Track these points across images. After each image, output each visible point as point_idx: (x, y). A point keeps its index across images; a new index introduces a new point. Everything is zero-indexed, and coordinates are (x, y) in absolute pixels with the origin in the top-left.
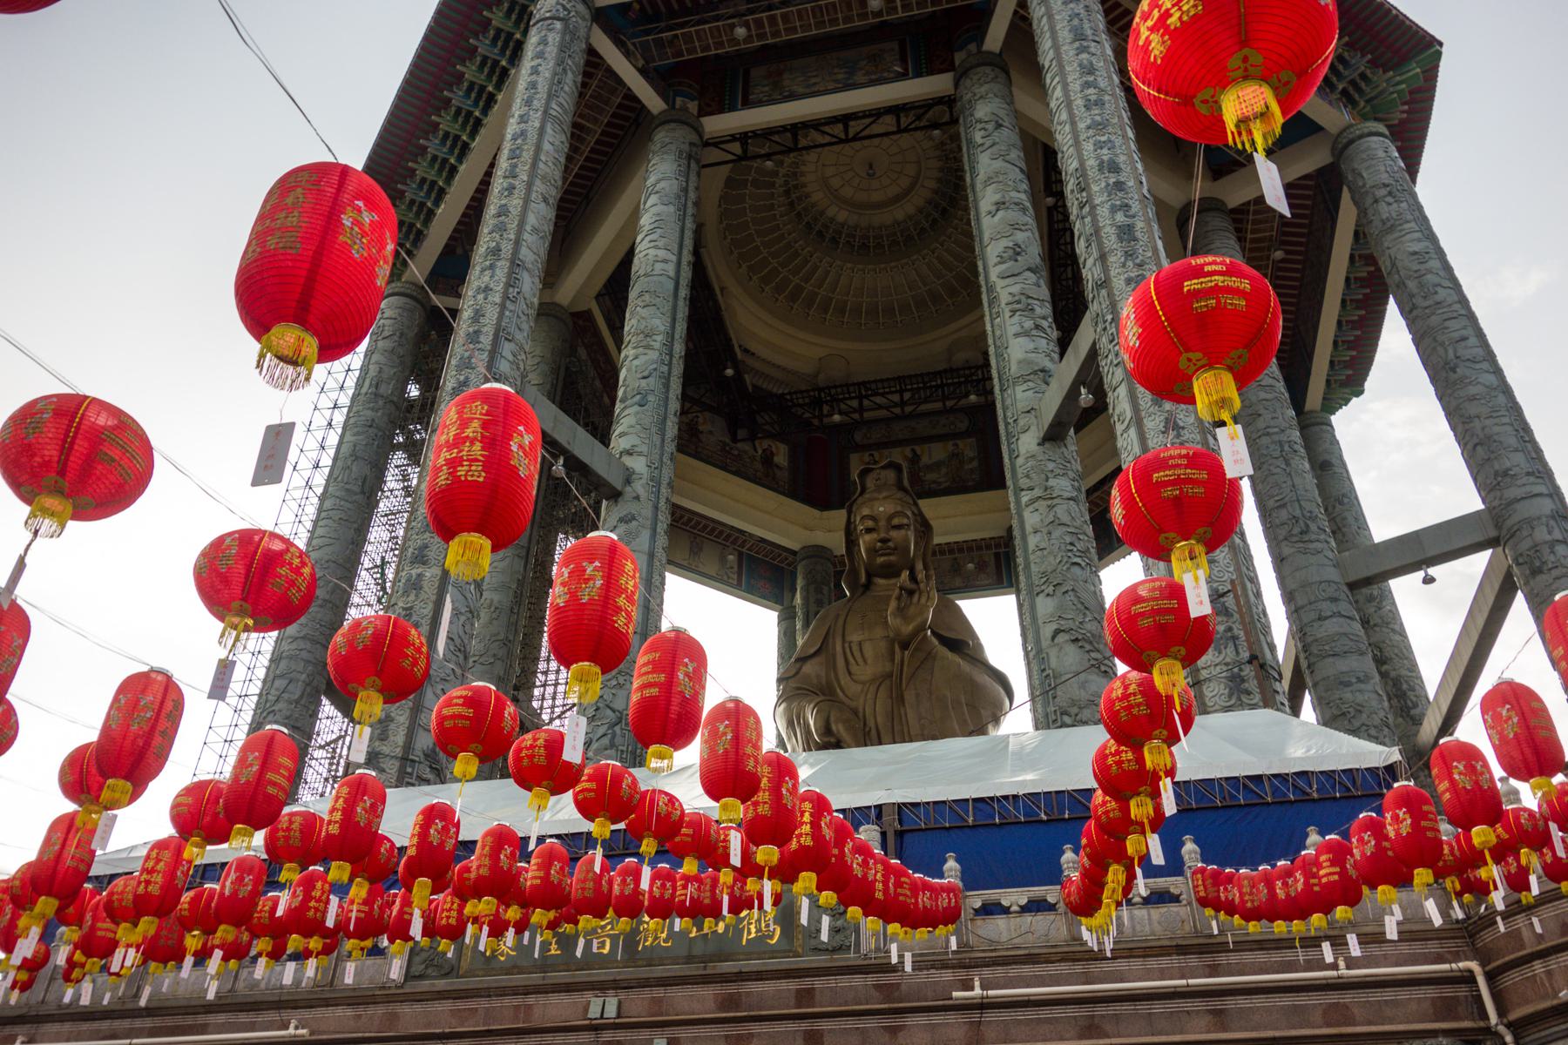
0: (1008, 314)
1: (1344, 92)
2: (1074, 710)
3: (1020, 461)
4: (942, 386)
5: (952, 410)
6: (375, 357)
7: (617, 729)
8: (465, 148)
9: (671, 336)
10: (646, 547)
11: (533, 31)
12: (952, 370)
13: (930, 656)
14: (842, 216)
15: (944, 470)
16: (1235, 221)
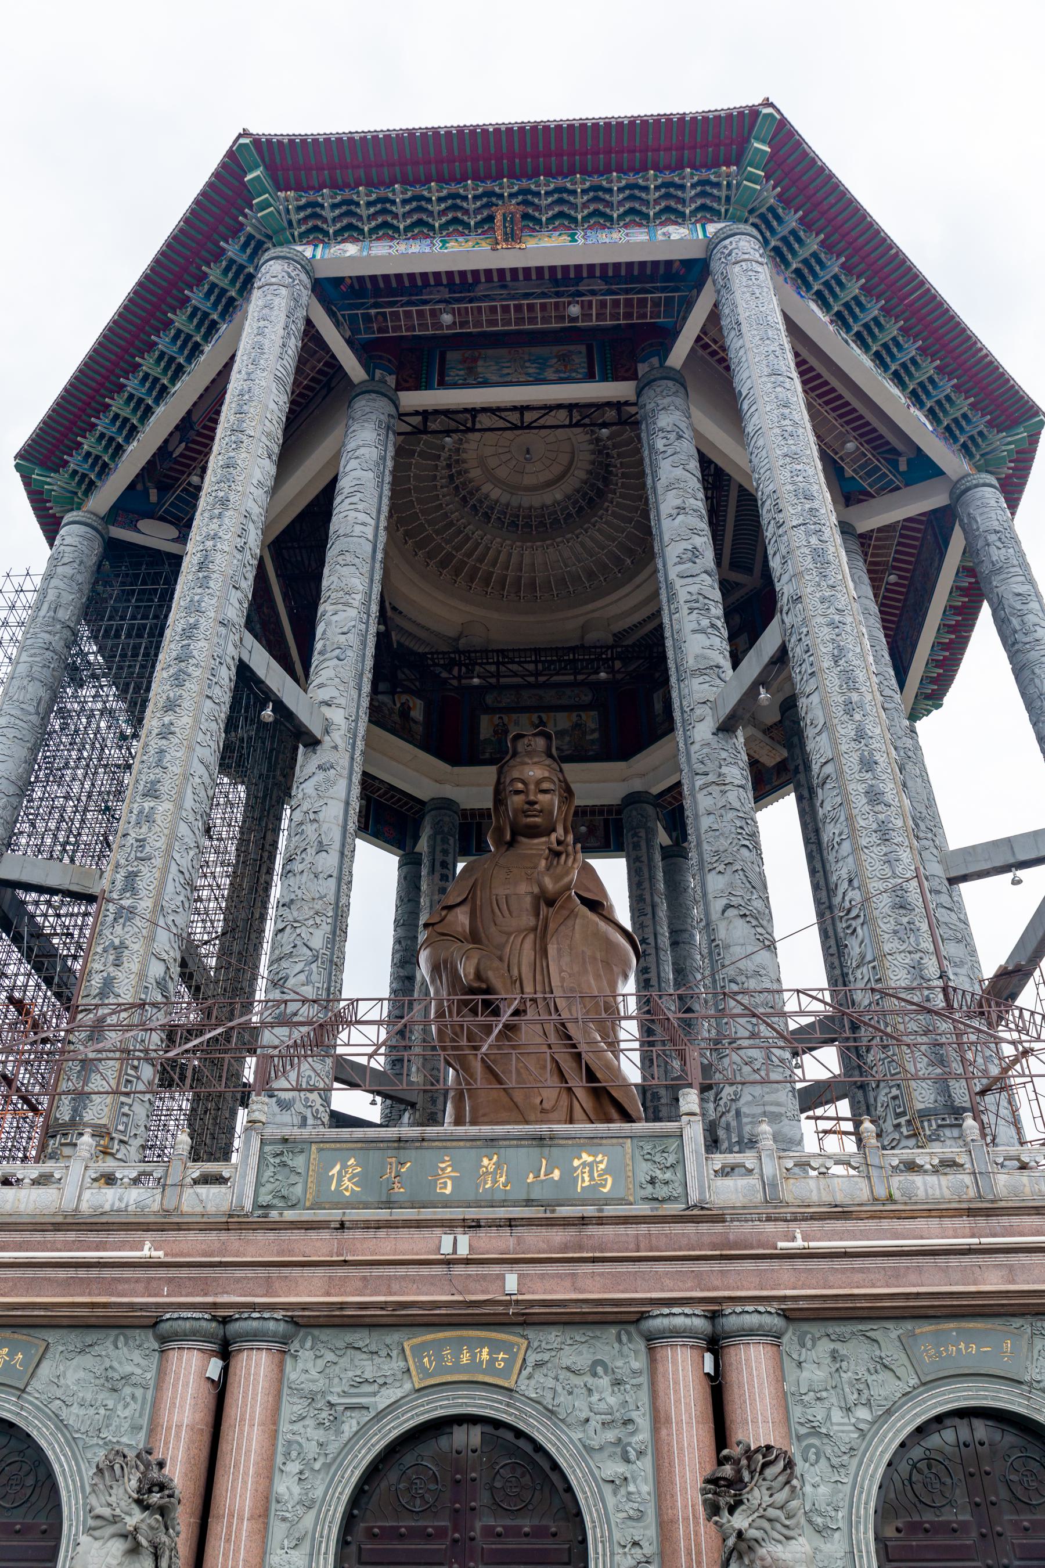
0: (686, 611)
1: (964, 446)
2: (739, 979)
3: (694, 748)
4: (574, 661)
5: (582, 684)
6: (54, 582)
7: (314, 966)
8: (164, 389)
9: (369, 595)
10: (343, 795)
11: (256, 294)
12: (582, 646)
13: (572, 914)
14: (495, 494)
15: (567, 739)
16: (862, 545)
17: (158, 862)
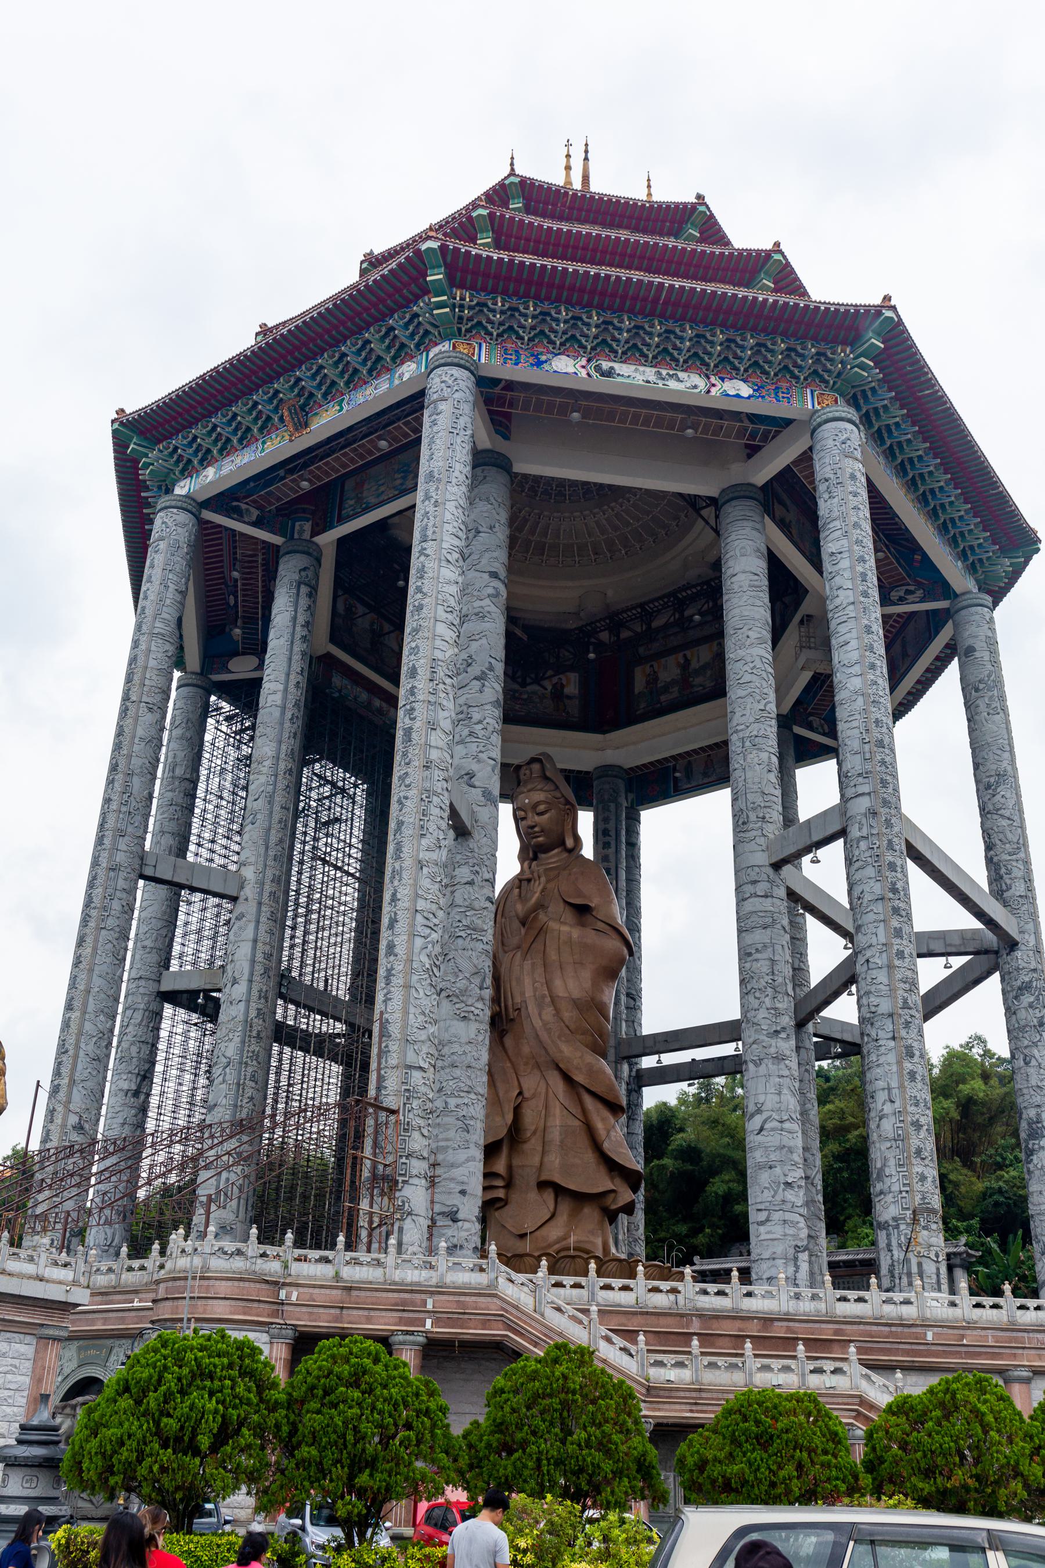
15: (709, 673)
17: (71, 1053)
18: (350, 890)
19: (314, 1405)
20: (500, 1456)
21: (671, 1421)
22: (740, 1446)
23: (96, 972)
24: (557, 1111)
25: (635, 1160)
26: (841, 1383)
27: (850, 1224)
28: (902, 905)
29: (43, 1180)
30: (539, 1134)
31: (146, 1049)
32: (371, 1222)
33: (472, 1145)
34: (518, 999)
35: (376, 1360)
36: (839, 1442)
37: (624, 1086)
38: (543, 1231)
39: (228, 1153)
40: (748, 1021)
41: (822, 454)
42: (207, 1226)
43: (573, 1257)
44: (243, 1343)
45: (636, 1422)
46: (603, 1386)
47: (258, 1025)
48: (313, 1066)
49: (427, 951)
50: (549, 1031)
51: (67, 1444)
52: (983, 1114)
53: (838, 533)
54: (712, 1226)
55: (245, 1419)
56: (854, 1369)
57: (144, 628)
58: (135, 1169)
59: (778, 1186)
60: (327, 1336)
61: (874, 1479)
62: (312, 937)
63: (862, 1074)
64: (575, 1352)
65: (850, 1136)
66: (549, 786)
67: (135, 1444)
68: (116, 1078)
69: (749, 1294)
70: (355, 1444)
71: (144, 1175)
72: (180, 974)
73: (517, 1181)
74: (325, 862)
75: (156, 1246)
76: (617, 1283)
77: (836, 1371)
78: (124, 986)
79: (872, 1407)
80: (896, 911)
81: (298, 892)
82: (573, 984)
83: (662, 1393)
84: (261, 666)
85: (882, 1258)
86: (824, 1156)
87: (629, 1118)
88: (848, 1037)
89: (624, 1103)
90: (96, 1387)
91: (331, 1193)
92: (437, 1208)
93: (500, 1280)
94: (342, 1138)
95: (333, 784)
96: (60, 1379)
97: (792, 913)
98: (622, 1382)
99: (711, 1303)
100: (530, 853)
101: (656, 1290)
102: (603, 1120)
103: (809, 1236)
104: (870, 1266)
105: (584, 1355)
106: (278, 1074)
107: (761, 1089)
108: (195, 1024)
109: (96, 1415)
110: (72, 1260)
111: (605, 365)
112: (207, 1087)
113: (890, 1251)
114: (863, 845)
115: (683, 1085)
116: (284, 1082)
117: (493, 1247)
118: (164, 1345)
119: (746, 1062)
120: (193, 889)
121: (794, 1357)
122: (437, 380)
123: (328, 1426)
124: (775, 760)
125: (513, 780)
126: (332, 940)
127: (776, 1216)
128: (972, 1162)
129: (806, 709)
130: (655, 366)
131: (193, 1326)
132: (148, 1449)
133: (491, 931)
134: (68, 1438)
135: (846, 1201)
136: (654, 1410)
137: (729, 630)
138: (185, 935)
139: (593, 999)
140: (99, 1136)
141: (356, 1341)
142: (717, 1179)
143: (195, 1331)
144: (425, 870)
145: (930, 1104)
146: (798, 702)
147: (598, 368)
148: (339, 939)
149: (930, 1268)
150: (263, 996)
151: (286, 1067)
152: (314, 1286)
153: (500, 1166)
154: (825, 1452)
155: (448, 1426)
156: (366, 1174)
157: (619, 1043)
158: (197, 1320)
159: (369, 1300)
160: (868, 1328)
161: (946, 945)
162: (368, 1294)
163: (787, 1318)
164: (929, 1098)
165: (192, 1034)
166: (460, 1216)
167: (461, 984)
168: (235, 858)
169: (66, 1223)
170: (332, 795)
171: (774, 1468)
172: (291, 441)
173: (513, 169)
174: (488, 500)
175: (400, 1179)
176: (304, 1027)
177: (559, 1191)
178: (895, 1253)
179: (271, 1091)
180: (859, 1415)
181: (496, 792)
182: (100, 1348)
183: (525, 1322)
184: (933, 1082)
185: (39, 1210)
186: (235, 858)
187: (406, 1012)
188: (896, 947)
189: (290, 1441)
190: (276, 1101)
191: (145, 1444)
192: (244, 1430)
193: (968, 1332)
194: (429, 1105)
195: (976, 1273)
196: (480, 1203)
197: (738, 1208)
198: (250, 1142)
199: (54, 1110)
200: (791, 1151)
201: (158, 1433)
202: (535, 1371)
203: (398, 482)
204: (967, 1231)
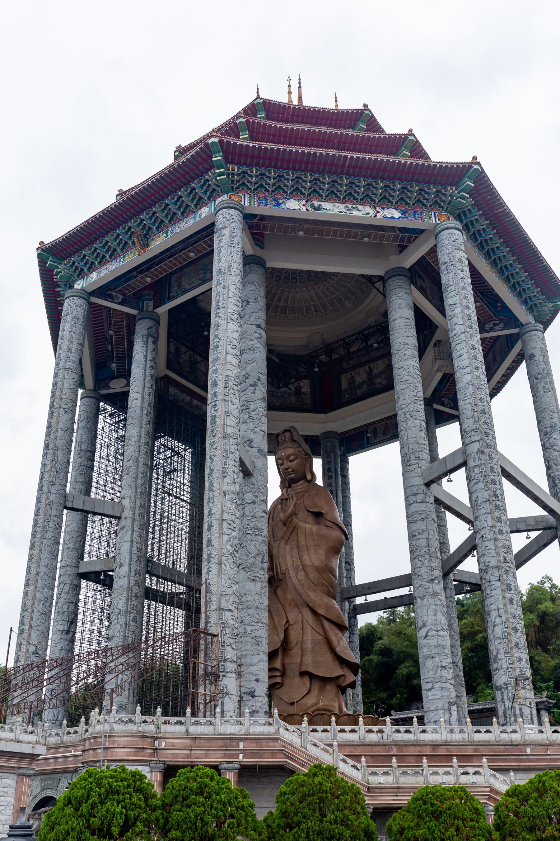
7: (119, 616)
18: (185, 510)
19: (178, 806)
20: (285, 831)
21: (382, 806)
22: (423, 819)
23: (42, 564)
24: (309, 631)
25: (355, 657)
26: (479, 780)
27: (480, 688)
28: (500, 504)
29: (16, 684)
30: (299, 644)
31: (72, 606)
32: (205, 700)
33: (261, 653)
34: (283, 568)
35: (212, 779)
36: (480, 814)
37: (346, 615)
38: (304, 701)
39: (122, 664)
40: (416, 574)
41: (442, 248)
42: (111, 706)
43: (322, 714)
44: (135, 772)
45: (363, 808)
46: (343, 788)
47: (135, 589)
48: (168, 611)
49: (230, 543)
50: (302, 585)
51: (37, 835)
52: (552, 621)
53: (453, 293)
54: (401, 693)
55: (138, 816)
56: (486, 771)
57: (61, 365)
58: (69, 676)
59: (438, 668)
60: (183, 767)
61: (501, 834)
62: (164, 538)
63: (482, 602)
64: (326, 769)
65: (477, 638)
66: (296, 445)
67: (76, 834)
68: (55, 624)
69: (424, 731)
70: (202, 828)
71: (74, 679)
72: (90, 562)
73: (288, 672)
74: (170, 494)
75: (83, 719)
76: (348, 728)
77: (475, 773)
78: (58, 571)
79: (497, 793)
80: (497, 507)
81: (155, 512)
82: (314, 558)
83: (376, 790)
84: (128, 384)
85: (499, 706)
86: (463, 650)
87: (350, 633)
88: (473, 581)
89: (347, 624)
90: (52, 802)
91: (182, 684)
92: (243, 690)
93: (281, 729)
94: (186, 652)
95: (172, 450)
96: (31, 798)
97: (438, 511)
98: (353, 785)
99: (402, 737)
100: (286, 484)
101: (370, 731)
102: (335, 635)
103: (457, 696)
104: (492, 712)
105: (331, 771)
106: (148, 617)
107: (425, 613)
108: (100, 591)
109: (53, 819)
110: (35, 730)
111: (316, 204)
112: (108, 626)
113: (503, 702)
114: (477, 470)
115: (381, 613)
116: (152, 622)
117: (276, 711)
118: (90, 776)
119: (415, 598)
120: (95, 514)
121: (451, 766)
122: (221, 217)
123: (186, 818)
124: (424, 424)
125: (274, 443)
126: (176, 539)
127: (437, 685)
128: (548, 649)
129: (440, 394)
130: (345, 203)
131: (106, 764)
132: (83, 836)
133: (266, 530)
134: (37, 832)
135: (476, 674)
136: (373, 800)
137: (394, 351)
138: (91, 540)
139: (326, 566)
140: (48, 658)
141: (200, 769)
142: (402, 666)
143: (107, 767)
144: (227, 496)
145: (522, 617)
146: (435, 391)
147: (312, 206)
148: (180, 538)
149: (526, 711)
150: (138, 573)
151: (153, 613)
152: (174, 738)
153: (278, 664)
154: (472, 820)
155: (255, 815)
156: (201, 672)
157: (343, 590)
158: (108, 761)
159: (206, 745)
160: (493, 747)
161: (527, 525)
162: (206, 741)
163: (446, 744)
164: (521, 613)
165: (98, 597)
166: (256, 694)
167: (251, 561)
168: (118, 495)
169: (31, 708)
170: (172, 456)
171: (443, 830)
172: (139, 255)
173: (258, 95)
174: (253, 283)
175: (221, 674)
176: (162, 589)
177: (312, 677)
178: (506, 703)
179: (144, 627)
180: (490, 798)
181: (266, 450)
182: (53, 779)
183: (296, 753)
184: (523, 604)
185: (15, 702)
186: (118, 495)
187: (220, 578)
188: (498, 528)
189: (165, 828)
190: (148, 633)
191: (82, 833)
192: (138, 823)
193: (550, 747)
194: (235, 631)
195: (553, 713)
196: (267, 686)
197: (415, 682)
198: (134, 657)
199: (21, 644)
200: (444, 647)
201: (89, 827)
202: (303, 781)
203: (202, 276)
204: (547, 689)
